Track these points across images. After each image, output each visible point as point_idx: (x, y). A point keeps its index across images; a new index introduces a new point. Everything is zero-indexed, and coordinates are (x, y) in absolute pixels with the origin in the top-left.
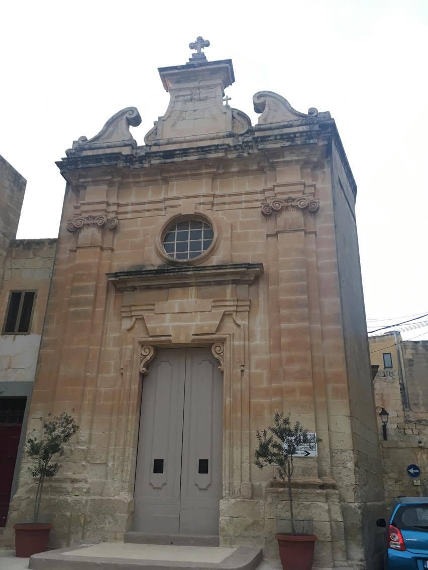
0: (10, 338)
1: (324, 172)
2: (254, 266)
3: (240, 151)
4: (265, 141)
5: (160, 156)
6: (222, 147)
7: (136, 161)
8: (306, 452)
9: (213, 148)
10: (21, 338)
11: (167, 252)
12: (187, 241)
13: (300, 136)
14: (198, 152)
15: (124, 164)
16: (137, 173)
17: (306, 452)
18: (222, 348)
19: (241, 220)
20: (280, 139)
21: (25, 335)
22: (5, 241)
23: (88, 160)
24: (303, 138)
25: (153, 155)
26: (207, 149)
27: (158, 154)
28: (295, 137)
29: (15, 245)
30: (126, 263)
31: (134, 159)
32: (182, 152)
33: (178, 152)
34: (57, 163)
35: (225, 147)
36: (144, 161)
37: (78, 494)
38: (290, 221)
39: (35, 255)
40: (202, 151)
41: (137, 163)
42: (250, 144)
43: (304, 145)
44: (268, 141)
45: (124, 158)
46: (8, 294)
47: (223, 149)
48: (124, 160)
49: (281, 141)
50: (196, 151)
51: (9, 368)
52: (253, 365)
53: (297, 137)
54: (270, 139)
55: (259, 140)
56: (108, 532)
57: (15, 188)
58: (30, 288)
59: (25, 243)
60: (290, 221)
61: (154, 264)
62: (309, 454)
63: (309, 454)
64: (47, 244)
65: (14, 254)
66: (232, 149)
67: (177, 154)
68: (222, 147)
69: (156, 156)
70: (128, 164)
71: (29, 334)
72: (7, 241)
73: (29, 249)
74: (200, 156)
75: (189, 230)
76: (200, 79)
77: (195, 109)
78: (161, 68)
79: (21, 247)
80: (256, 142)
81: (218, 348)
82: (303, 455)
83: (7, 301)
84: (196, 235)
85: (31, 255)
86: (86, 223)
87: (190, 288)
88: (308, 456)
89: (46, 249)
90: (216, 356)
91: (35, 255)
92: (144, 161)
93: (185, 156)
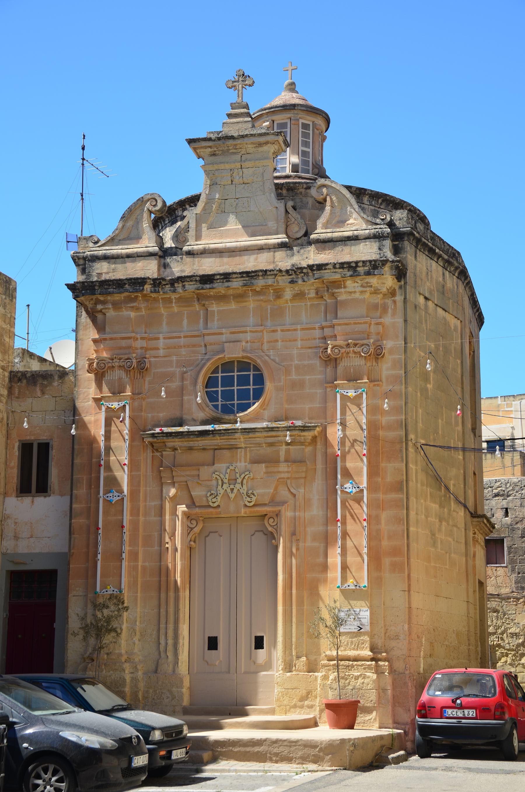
0: (27, 500)
1: (395, 302)
2: (310, 428)
3: (294, 276)
4: (322, 269)
5: (196, 281)
6: (272, 273)
7: (167, 284)
8: (359, 627)
9: (261, 274)
10: (41, 501)
11: (210, 402)
12: (233, 388)
13: (363, 266)
14: (242, 277)
15: (153, 288)
16: (168, 296)
17: (359, 627)
18: (276, 519)
19: (296, 362)
20: (340, 268)
21: (45, 497)
22: (4, 376)
23: (106, 285)
24: (367, 268)
25: (188, 280)
26: (253, 274)
27: (194, 279)
28: (357, 266)
29: (16, 379)
30: (161, 415)
31: (164, 283)
32: (223, 277)
33: (218, 277)
34: (69, 286)
35: (275, 272)
36: (176, 285)
37: (133, 671)
38: (352, 370)
39: (43, 393)
40: (248, 276)
41: (167, 286)
42: (305, 271)
43: (368, 273)
44: (325, 269)
45: (152, 282)
46: (17, 445)
47: (272, 275)
48: (151, 284)
49: (341, 270)
50: (239, 276)
51: (32, 537)
52: (309, 538)
53: (360, 267)
54: (327, 267)
55: (314, 268)
56: (166, 706)
57: (7, 301)
58: (44, 438)
59: (28, 375)
60: (352, 370)
61: (195, 418)
62: (361, 629)
63: (361, 629)
64: (56, 377)
65: (17, 391)
66: (284, 274)
67: (217, 279)
68: (272, 273)
69: (191, 281)
70: (157, 289)
71: (50, 496)
72: (7, 374)
73: (35, 383)
74: (245, 282)
75: (236, 374)
76: (242, 153)
77: (237, 197)
78: (190, 139)
79: (25, 381)
80: (312, 270)
81: (271, 520)
82: (356, 630)
83: (17, 454)
84: (244, 380)
85: (39, 393)
86: (110, 365)
87: (239, 450)
88: (361, 631)
89: (55, 384)
90: (270, 529)
91: (43, 393)
92: (176, 285)
93: (227, 281)
